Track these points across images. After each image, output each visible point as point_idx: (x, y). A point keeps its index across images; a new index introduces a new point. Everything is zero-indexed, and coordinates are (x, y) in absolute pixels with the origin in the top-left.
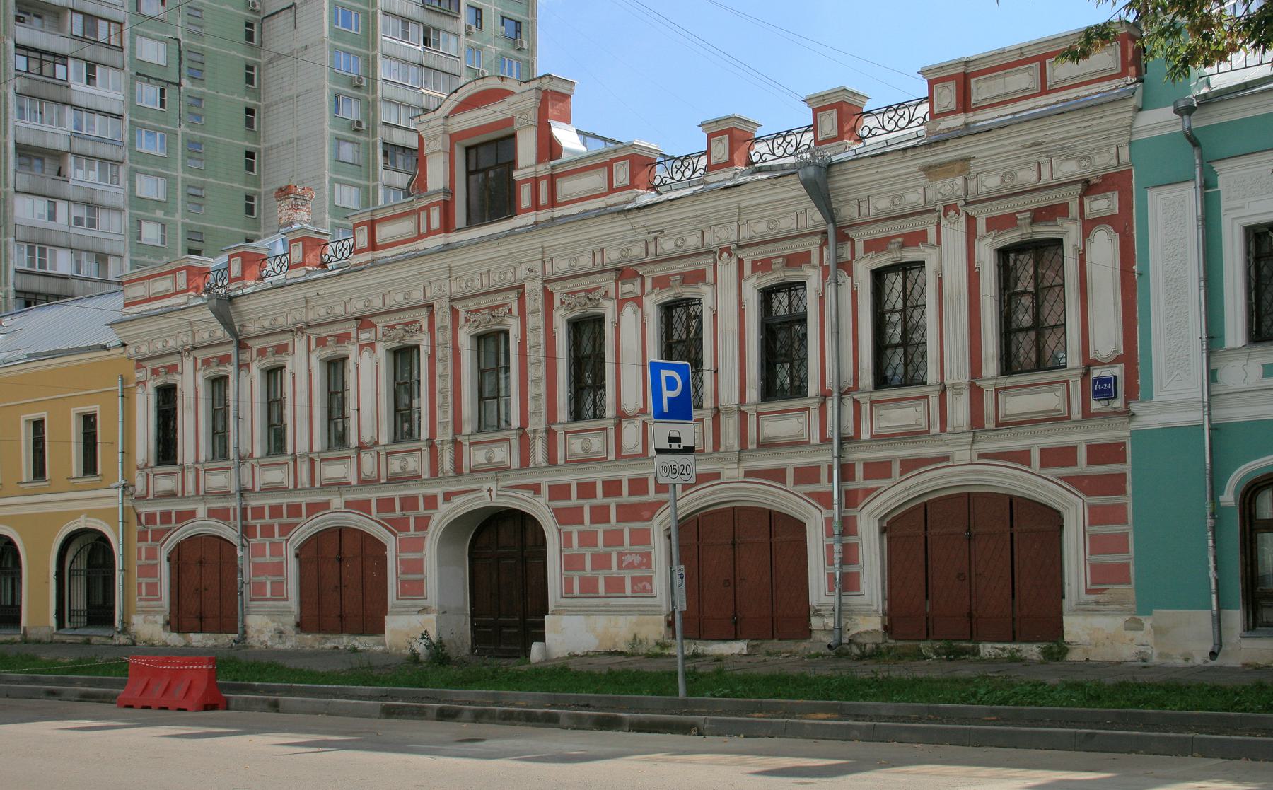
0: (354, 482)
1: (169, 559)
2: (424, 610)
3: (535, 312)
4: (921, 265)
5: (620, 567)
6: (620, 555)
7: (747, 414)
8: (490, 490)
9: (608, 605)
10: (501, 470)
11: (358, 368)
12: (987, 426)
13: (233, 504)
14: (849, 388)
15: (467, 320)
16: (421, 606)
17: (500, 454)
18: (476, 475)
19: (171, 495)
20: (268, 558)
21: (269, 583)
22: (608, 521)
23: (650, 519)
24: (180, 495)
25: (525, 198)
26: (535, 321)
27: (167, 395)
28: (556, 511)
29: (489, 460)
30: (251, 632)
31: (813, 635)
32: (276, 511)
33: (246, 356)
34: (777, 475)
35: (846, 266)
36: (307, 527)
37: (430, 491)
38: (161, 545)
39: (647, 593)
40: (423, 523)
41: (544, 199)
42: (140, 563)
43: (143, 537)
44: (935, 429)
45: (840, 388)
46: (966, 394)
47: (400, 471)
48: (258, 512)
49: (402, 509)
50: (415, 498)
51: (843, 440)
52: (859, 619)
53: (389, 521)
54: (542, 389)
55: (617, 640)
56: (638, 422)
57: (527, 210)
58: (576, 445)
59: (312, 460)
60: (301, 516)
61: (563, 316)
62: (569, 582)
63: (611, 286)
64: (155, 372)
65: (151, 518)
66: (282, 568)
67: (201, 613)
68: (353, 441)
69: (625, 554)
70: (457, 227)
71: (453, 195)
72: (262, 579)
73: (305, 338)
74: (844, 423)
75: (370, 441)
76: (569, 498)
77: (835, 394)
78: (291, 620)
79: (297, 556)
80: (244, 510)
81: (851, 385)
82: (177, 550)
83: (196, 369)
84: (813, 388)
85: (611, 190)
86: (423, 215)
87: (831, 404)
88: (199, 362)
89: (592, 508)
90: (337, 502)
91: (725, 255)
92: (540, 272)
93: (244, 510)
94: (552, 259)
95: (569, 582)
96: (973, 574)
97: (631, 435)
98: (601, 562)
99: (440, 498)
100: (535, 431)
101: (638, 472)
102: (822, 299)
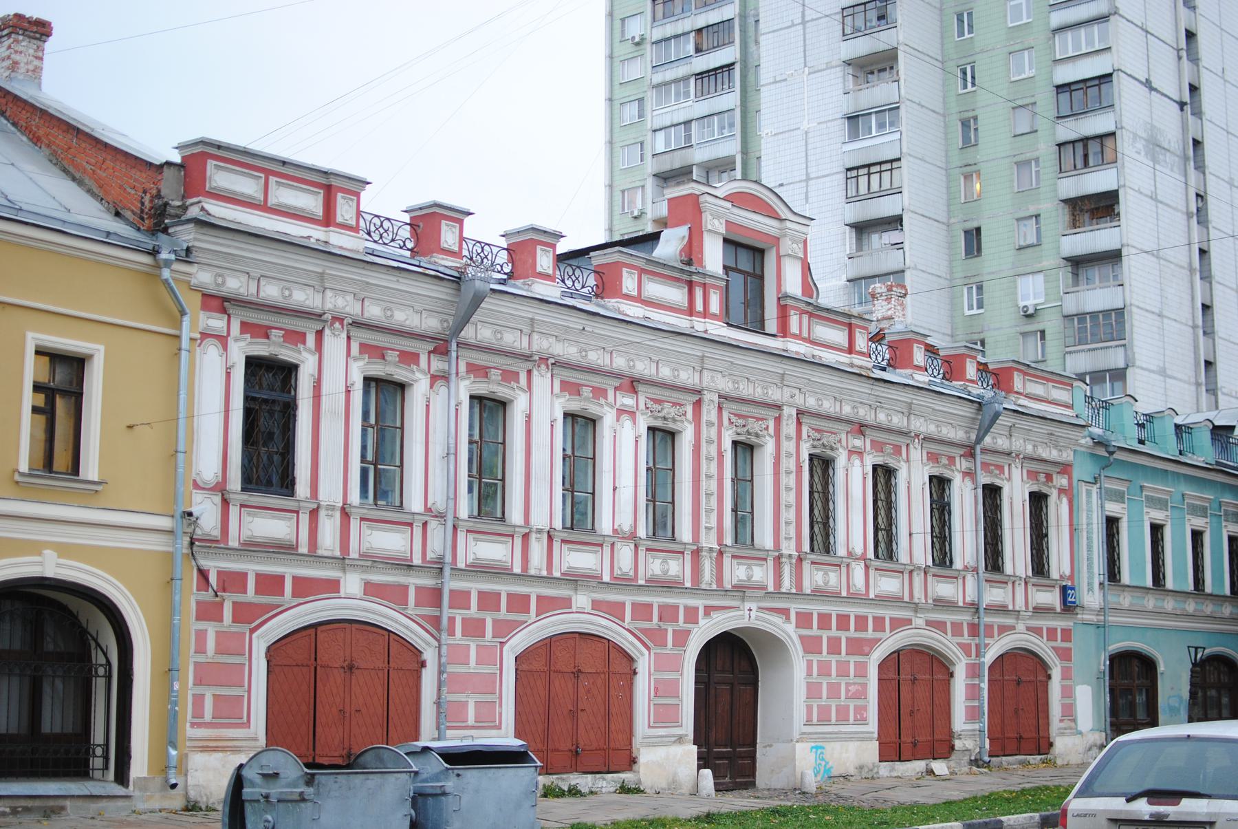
2: (680, 740)
3: (789, 438)
9: (840, 733)
18: (749, 593)
19: (285, 549)
24: (304, 549)
26: (788, 446)
28: (801, 637)
32: (489, 601)
38: (252, 631)
40: (682, 638)
42: (201, 658)
43: (208, 612)
47: (660, 573)
48: (461, 599)
49: (660, 619)
53: (643, 631)
59: (550, 538)
62: (809, 708)
65: (232, 581)
72: (461, 698)
90: (582, 600)
98: (834, 691)
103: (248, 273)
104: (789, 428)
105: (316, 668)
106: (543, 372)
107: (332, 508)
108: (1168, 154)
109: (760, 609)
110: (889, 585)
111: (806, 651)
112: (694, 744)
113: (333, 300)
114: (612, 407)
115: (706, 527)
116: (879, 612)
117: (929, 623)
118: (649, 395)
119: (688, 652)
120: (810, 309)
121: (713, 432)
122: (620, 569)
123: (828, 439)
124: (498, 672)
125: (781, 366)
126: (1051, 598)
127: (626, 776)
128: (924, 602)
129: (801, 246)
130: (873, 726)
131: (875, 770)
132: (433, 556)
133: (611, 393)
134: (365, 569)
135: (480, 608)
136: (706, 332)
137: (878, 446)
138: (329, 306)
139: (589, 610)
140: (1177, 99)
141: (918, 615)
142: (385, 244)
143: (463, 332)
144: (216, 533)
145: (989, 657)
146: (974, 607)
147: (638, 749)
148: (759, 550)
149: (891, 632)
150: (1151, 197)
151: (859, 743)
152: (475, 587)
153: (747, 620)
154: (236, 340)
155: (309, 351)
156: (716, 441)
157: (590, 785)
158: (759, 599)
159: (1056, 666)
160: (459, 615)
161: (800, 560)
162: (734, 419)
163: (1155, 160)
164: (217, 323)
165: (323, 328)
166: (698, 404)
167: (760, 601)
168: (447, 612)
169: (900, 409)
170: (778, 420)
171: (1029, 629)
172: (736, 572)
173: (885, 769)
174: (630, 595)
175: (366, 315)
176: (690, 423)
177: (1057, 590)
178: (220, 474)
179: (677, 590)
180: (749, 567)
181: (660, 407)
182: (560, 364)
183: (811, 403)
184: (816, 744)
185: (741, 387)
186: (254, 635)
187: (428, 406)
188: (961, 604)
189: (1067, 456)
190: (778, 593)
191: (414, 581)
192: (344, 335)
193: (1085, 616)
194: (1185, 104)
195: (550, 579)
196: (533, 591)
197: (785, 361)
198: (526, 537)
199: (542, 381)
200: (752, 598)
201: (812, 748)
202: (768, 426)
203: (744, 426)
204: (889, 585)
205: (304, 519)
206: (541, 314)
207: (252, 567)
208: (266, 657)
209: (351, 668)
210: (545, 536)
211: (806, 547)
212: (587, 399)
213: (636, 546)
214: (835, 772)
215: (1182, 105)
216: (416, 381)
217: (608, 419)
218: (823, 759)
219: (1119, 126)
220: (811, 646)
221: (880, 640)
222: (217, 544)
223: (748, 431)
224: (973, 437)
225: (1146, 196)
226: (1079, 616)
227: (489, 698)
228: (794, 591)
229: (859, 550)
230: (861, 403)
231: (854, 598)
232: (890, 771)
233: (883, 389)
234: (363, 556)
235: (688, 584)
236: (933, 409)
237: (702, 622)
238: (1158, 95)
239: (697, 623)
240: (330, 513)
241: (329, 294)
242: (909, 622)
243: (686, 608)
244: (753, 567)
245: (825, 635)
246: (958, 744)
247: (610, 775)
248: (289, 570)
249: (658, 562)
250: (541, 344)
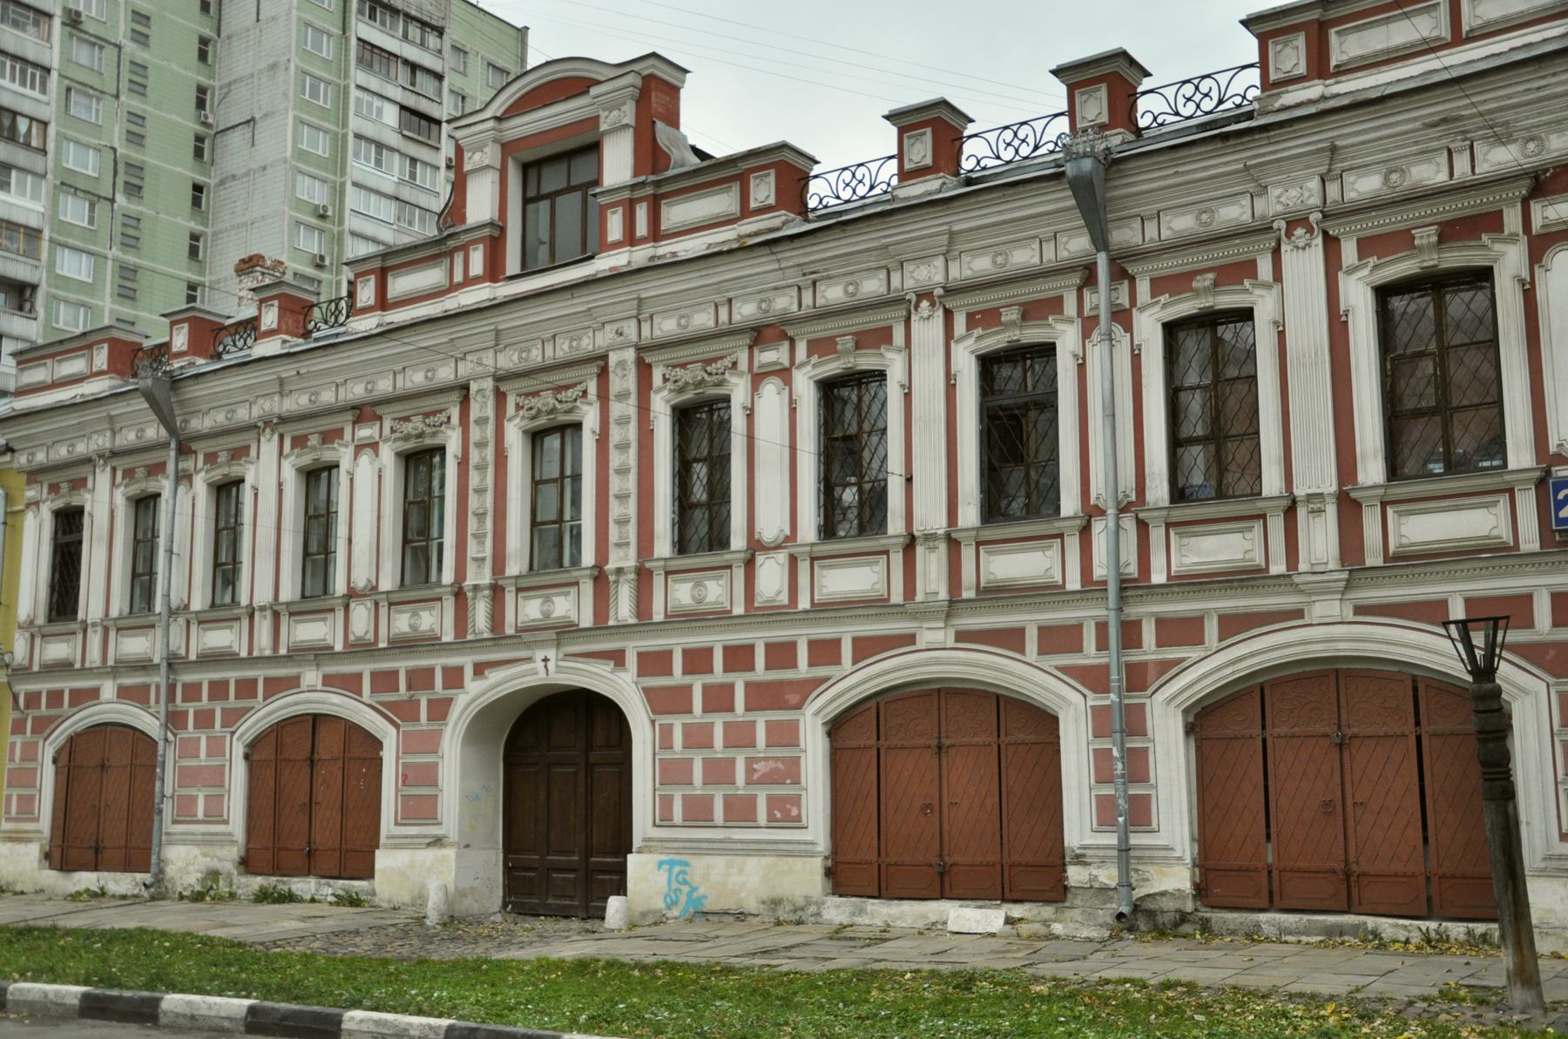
0: (339, 647)
1: (55, 761)
2: (438, 842)
3: (623, 396)
4: (1246, 315)
5: (749, 782)
6: (750, 762)
7: (959, 543)
8: (546, 660)
10: (565, 631)
11: (352, 480)
12: (1370, 561)
13: (159, 679)
14: (1129, 503)
15: (518, 407)
16: (433, 836)
17: (563, 607)
18: (527, 637)
22: (731, 709)
23: (799, 706)
25: (615, 227)
26: (623, 409)
27: (69, 522)
28: (648, 692)
29: (547, 615)
30: (171, 871)
31: (1069, 896)
32: (219, 689)
33: (187, 464)
34: (1011, 639)
35: (1122, 317)
36: (265, 714)
37: (453, 661)
38: (46, 739)
39: (796, 822)
40: (440, 710)
41: (642, 228)
42: (12, 766)
43: (18, 728)
44: (1279, 567)
45: (1118, 503)
46: (1331, 510)
48: (192, 692)
49: (409, 688)
50: (430, 671)
51: (1125, 585)
52: (1151, 870)
54: (631, 508)
55: (743, 895)
56: (782, 557)
57: (616, 245)
58: (683, 594)
60: (255, 696)
61: (668, 401)
62: (667, 802)
63: (743, 358)
65: (32, 699)
66: (222, 775)
67: (97, 841)
68: (340, 587)
69: (758, 760)
70: (508, 274)
71: (503, 229)
72: (192, 791)
73: (276, 437)
74: (1123, 559)
75: (365, 588)
76: (669, 672)
77: (1111, 511)
78: (233, 853)
79: (247, 757)
80: (171, 689)
81: (1133, 497)
82: (67, 749)
83: (113, 484)
84: (1070, 504)
85: (746, 212)
86: (459, 259)
87: (1101, 532)
88: (119, 474)
89: (706, 689)
90: (311, 677)
91: (925, 304)
92: (634, 338)
93: (171, 689)
94: (651, 317)
95: (667, 802)
96: (1349, 803)
97: (771, 577)
98: (719, 772)
99: (468, 672)
100: (619, 571)
101: (780, 634)
102: (1082, 368)
104: (624, 380)
106: (268, 436)
118: (395, 416)
120: (649, 191)
124: (228, 764)
125: (576, 301)
127: (358, 885)
131: (813, 909)
139: (319, 687)
149: (855, 661)
152: (205, 677)
153: (542, 674)
157: (313, 891)
162: (521, 400)
169: (874, 265)
170: (603, 374)
173: (837, 911)
174: (370, 662)
180: (698, 584)
183: (667, 326)
184: (671, 857)
195: (274, 659)
196: (260, 673)
197: (577, 293)
201: (661, 863)
207: (44, 686)
214: (710, 904)
218: (685, 882)
220: (665, 702)
221: (827, 679)
222: (23, 672)
228: (632, 621)
230: (776, 288)
231: (758, 613)
232: (853, 914)
233: (801, 251)
242: (910, 639)
243: (445, 670)
246: (1075, 875)
247: (341, 882)
248: (66, 685)
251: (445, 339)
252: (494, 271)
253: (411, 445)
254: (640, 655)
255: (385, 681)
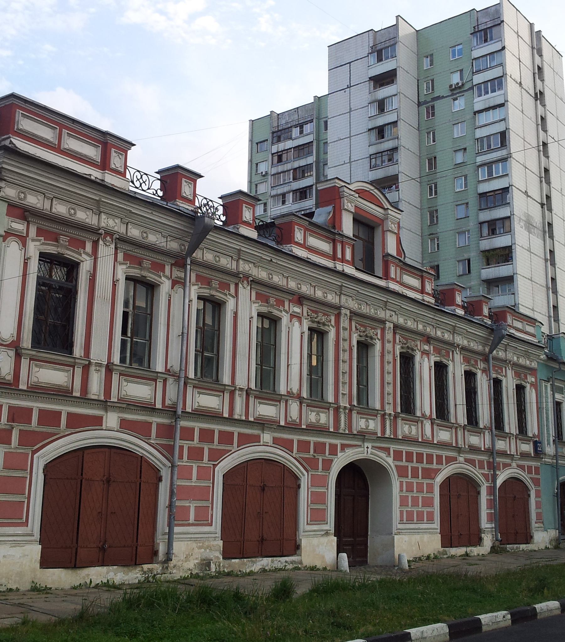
3: (389, 342)
8: (368, 448)
20: (194, 482)
21: (192, 506)
24: (77, 394)
28: (396, 466)
29: (367, 428)
32: (206, 435)
38: (34, 452)
40: (328, 465)
47: (315, 421)
48: (188, 434)
49: (315, 452)
53: (305, 459)
59: (248, 395)
62: (402, 512)
64: (40, 232)
90: (267, 437)
103: (44, 194)
104: (389, 336)
105: (81, 481)
107: (100, 365)
108: (536, 229)
109: (373, 447)
110: (444, 436)
111: (400, 476)
112: (335, 536)
113: (106, 221)
114: (287, 312)
115: (342, 393)
116: (439, 452)
117: (467, 460)
119: (331, 474)
121: (347, 334)
122: (291, 417)
123: (411, 344)
124: (211, 485)
126: (527, 448)
128: (463, 447)
129: (396, 226)
130: (437, 525)
132: (170, 403)
133: (286, 304)
134: (121, 409)
135: (201, 440)
136: (343, 270)
137: (438, 351)
138: (103, 224)
139: (271, 443)
140: (540, 202)
141: (461, 455)
142: (143, 190)
143: (194, 254)
144: (10, 378)
145: (499, 482)
146: (491, 452)
147: (301, 540)
148: (371, 409)
149: (446, 465)
150: (528, 250)
151: (430, 535)
152: (197, 425)
153: (365, 454)
154: (33, 240)
155: (87, 254)
156: (348, 339)
158: (373, 441)
159: (533, 489)
160: (186, 444)
161: (396, 417)
162: (359, 327)
163: (530, 232)
164: (19, 226)
165: (98, 239)
166: (338, 316)
167: (373, 442)
168: (179, 443)
170: (383, 330)
171: (518, 466)
172: (360, 423)
175: (129, 234)
176: (333, 327)
177: (532, 443)
178: (15, 335)
179: (325, 433)
181: (316, 315)
182: (255, 282)
183: (401, 321)
185: (363, 307)
186: (35, 456)
187: (169, 300)
188: (483, 449)
189: (534, 365)
190: (383, 438)
191: (156, 420)
192: (113, 246)
193: (546, 460)
194: (544, 204)
195: (246, 423)
196: (236, 430)
198: (232, 393)
199: (245, 292)
200: (369, 440)
202: (377, 333)
203: (364, 332)
204: (444, 436)
205: (78, 371)
206: (246, 248)
208: (44, 472)
209: (108, 481)
210: (245, 393)
211: (399, 410)
212: (272, 306)
213: (301, 403)
215: (542, 205)
216: (162, 283)
217: (285, 319)
219: (512, 214)
220: (402, 471)
223: (366, 335)
224: (487, 350)
225: (526, 249)
226: (543, 460)
227: (204, 504)
229: (428, 413)
230: (428, 324)
234: (121, 400)
235: (332, 430)
236: (467, 331)
237: (339, 454)
238: (531, 199)
239: (337, 455)
240: (98, 368)
241: (103, 216)
242: (455, 459)
244: (369, 420)
245: (410, 465)
249: (314, 414)
250: (244, 267)
251: (340, 284)
252: (352, 263)
253: (315, 325)
254: (394, 451)
255: (304, 446)
